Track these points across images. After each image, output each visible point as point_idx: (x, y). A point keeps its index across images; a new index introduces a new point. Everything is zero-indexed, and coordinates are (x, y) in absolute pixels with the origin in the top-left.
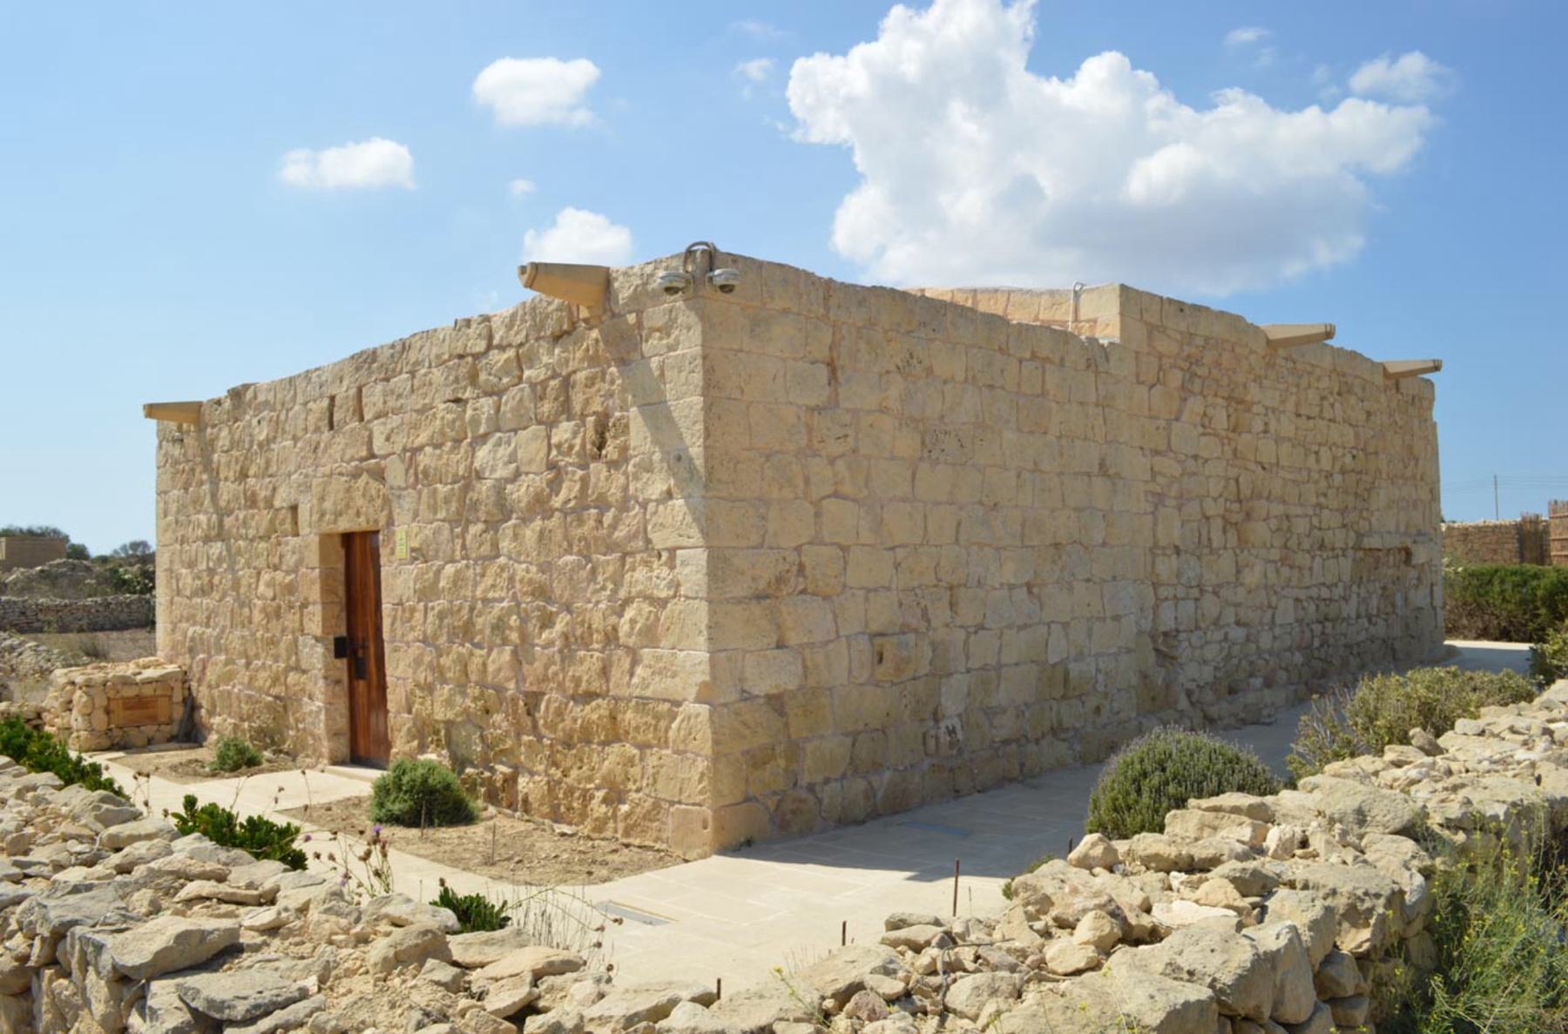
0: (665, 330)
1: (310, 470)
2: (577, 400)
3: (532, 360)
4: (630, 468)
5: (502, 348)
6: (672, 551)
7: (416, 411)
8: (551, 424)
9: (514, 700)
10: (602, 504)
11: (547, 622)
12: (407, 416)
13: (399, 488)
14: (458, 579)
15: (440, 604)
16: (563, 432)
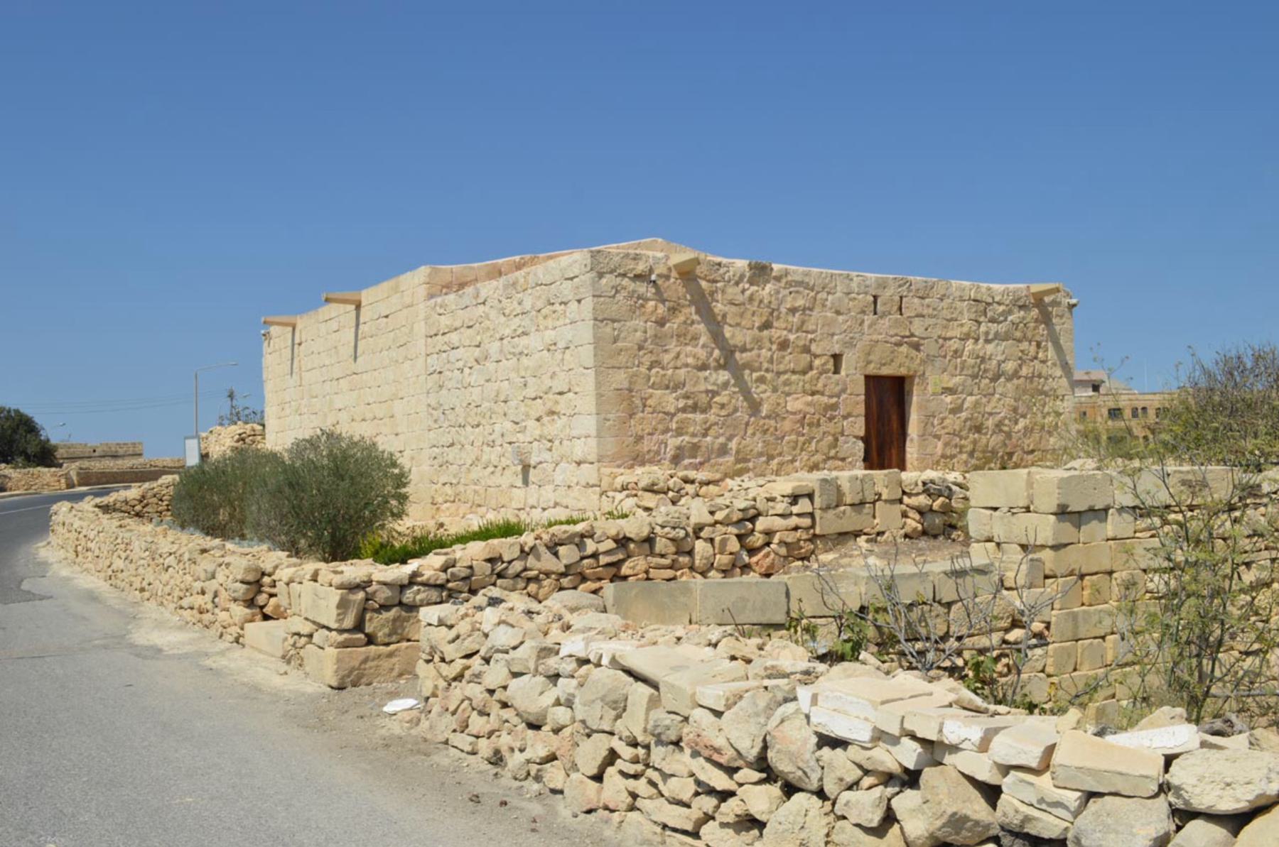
0: (1061, 317)
1: (857, 335)
2: (1029, 334)
3: (1010, 312)
4: (1049, 363)
5: (999, 303)
6: (1063, 396)
7: (947, 320)
8: (1019, 341)
9: (1002, 457)
10: (1040, 376)
11: (1016, 423)
12: (939, 321)
13: (934, 356)
14: (977, 404)
15: (964, 415)
16: (1025, 345)
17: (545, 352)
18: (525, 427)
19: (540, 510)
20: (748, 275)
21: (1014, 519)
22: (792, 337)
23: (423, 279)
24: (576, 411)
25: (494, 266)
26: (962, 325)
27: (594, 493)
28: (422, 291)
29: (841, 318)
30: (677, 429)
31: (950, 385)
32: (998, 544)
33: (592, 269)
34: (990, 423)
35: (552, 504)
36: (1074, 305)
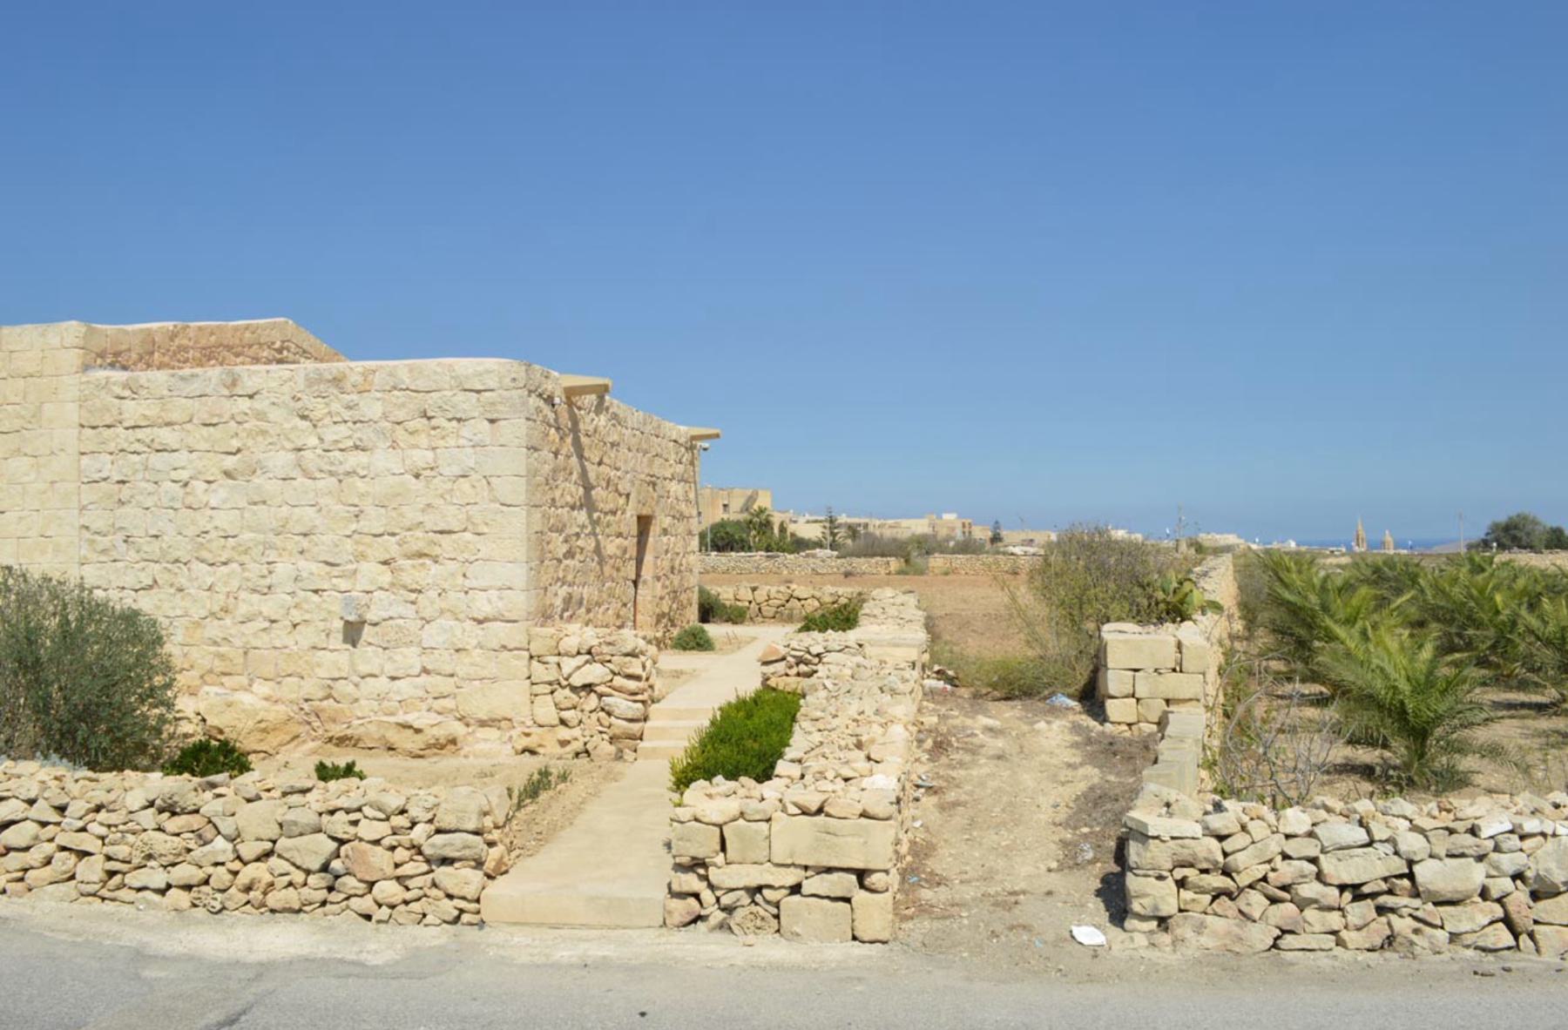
17: (409, 477)
18: (355, 571)
19: (384, 680)
20: (595, 403)
21: (1160, 679)
22: (612, 474)
23: (70, 340)
24: (480, 555)
25: (149, 332)
26: (671, 465)
27: (518, 658)
28: (73, 358)
29: (630, 454)
30: (564, 577)
31: (665, 526)
32: (1138, 700)
33: (525, 386)
34: (677, 563)
35: (417, 670)
36: (705, 449)
